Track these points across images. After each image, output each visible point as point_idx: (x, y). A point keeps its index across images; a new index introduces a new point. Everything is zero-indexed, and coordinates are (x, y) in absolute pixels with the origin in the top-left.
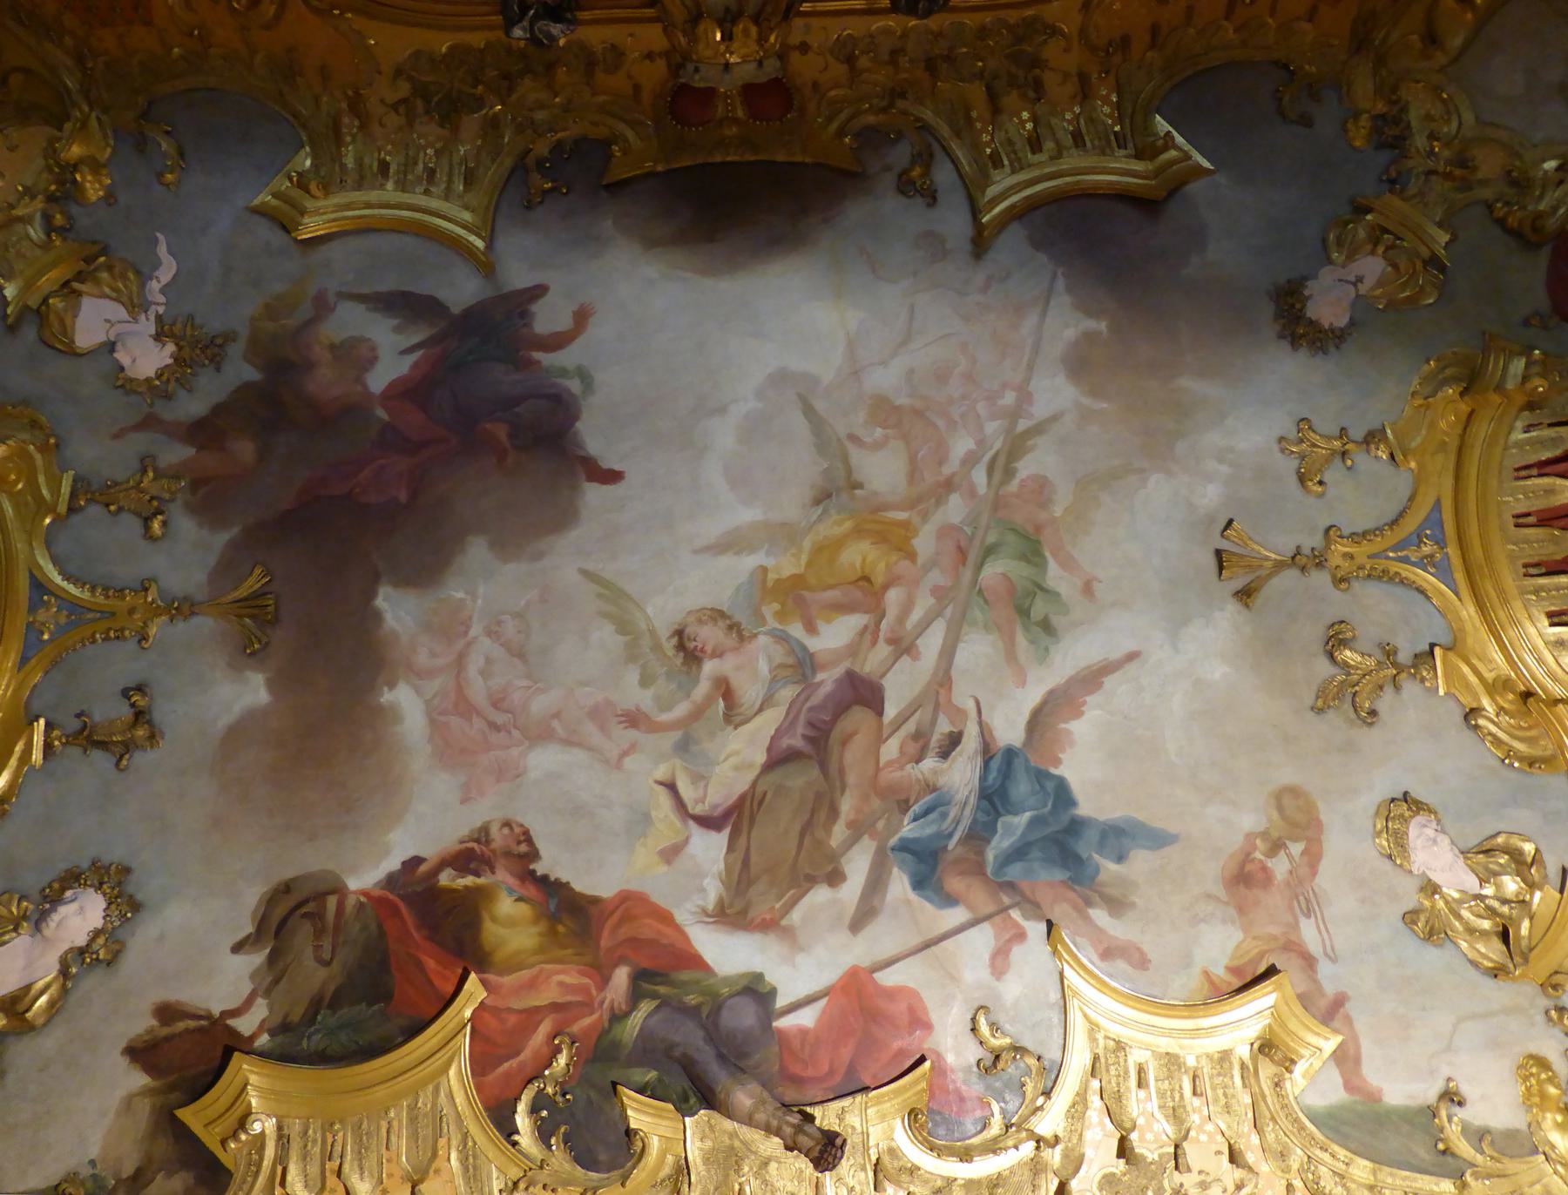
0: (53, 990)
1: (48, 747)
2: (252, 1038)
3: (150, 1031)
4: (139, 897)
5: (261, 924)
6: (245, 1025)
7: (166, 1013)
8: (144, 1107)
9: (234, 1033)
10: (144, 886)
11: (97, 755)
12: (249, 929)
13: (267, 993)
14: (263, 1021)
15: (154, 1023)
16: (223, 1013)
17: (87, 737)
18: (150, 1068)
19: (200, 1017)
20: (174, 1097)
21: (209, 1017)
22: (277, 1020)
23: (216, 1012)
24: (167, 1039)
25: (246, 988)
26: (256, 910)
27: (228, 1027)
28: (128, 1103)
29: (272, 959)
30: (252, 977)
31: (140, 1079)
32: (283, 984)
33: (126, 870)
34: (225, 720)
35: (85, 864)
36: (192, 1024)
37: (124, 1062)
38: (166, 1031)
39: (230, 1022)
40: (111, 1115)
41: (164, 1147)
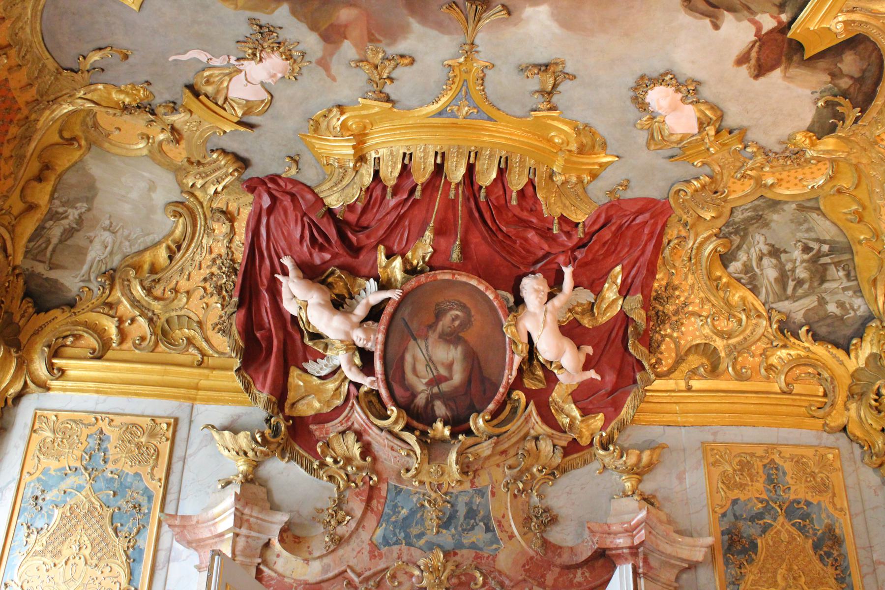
0: (703, 107)
1: (550, 109)
2: (780, 22)
3: (750, 68)
4: (662, 71)
5: (705, 14)
6: (768, 23)
7: (742, 60)
8: (794, 71)
9: (771, 32)
10: (656, 67)
11: (560, 88)
12: (707, 21)
13: (754, 13)
14: (772, 16)
15: (745, 66)
16: (755, 36)
17: (548, 94)
18: (772, 68)
19: (753, 46)
20: (795, 58)
21: (755, 42)
22: (775, 10)
23: (754, 38)
24: (758, 60)
25: (746, 24)
26: (696, 17)
27: (766, 34)
28: (785, 77)
29: (731, 9)
30: (739, 20)
31: (777, 73)
32: (752, 7)
33: (642, 77)
34: (555, 28)
35: (632, 94)
36: (755, 49)
37: (762, 80)
38: (753, 62)
39: (763, 32)
40: (791, 85)
41: (822, 64)
